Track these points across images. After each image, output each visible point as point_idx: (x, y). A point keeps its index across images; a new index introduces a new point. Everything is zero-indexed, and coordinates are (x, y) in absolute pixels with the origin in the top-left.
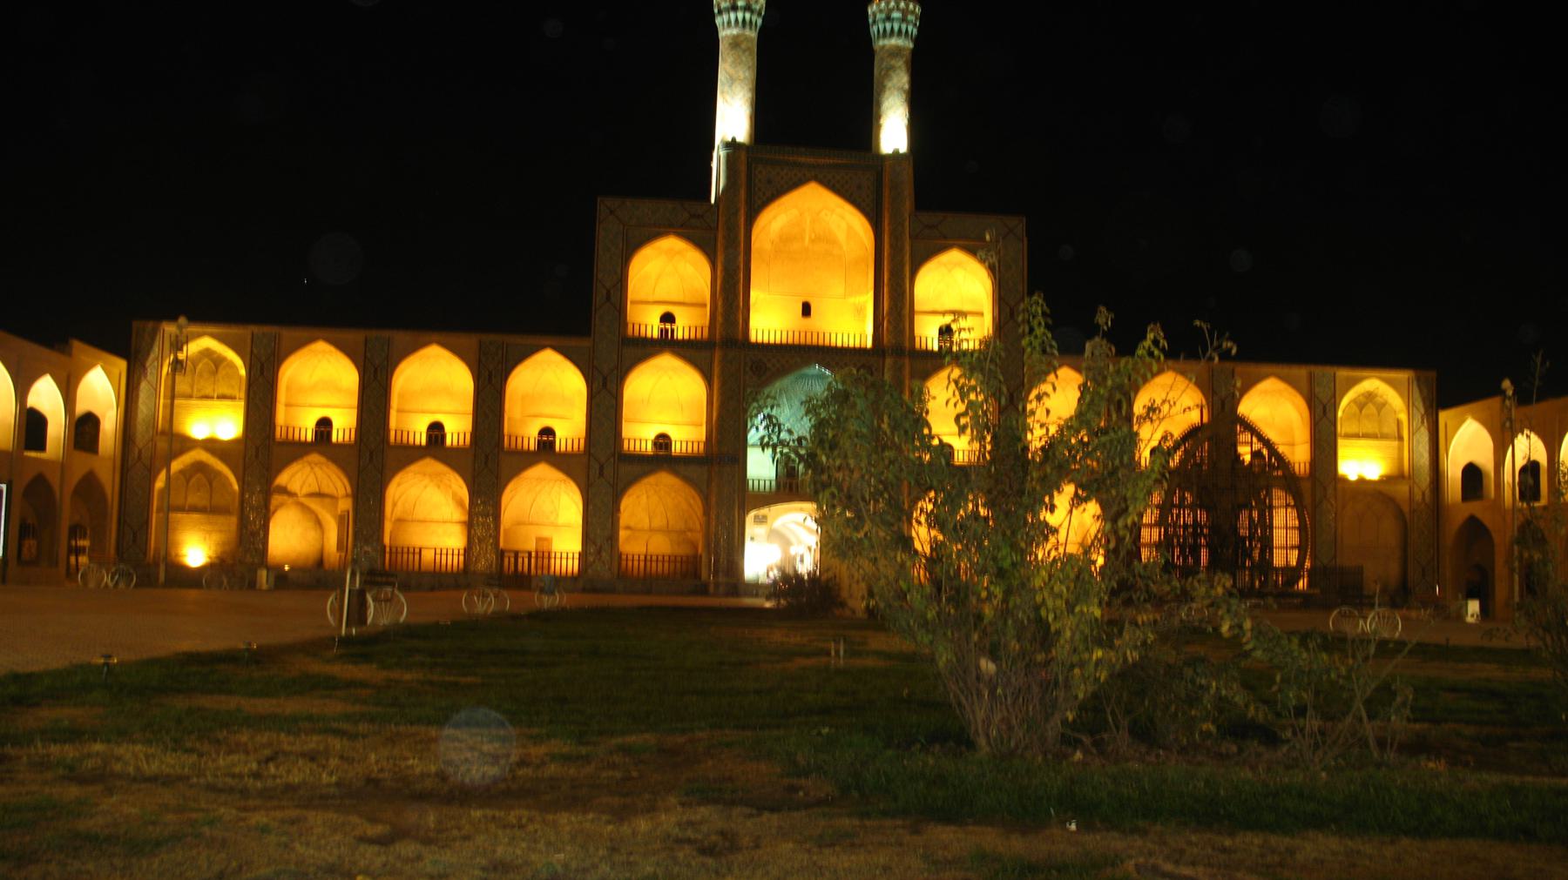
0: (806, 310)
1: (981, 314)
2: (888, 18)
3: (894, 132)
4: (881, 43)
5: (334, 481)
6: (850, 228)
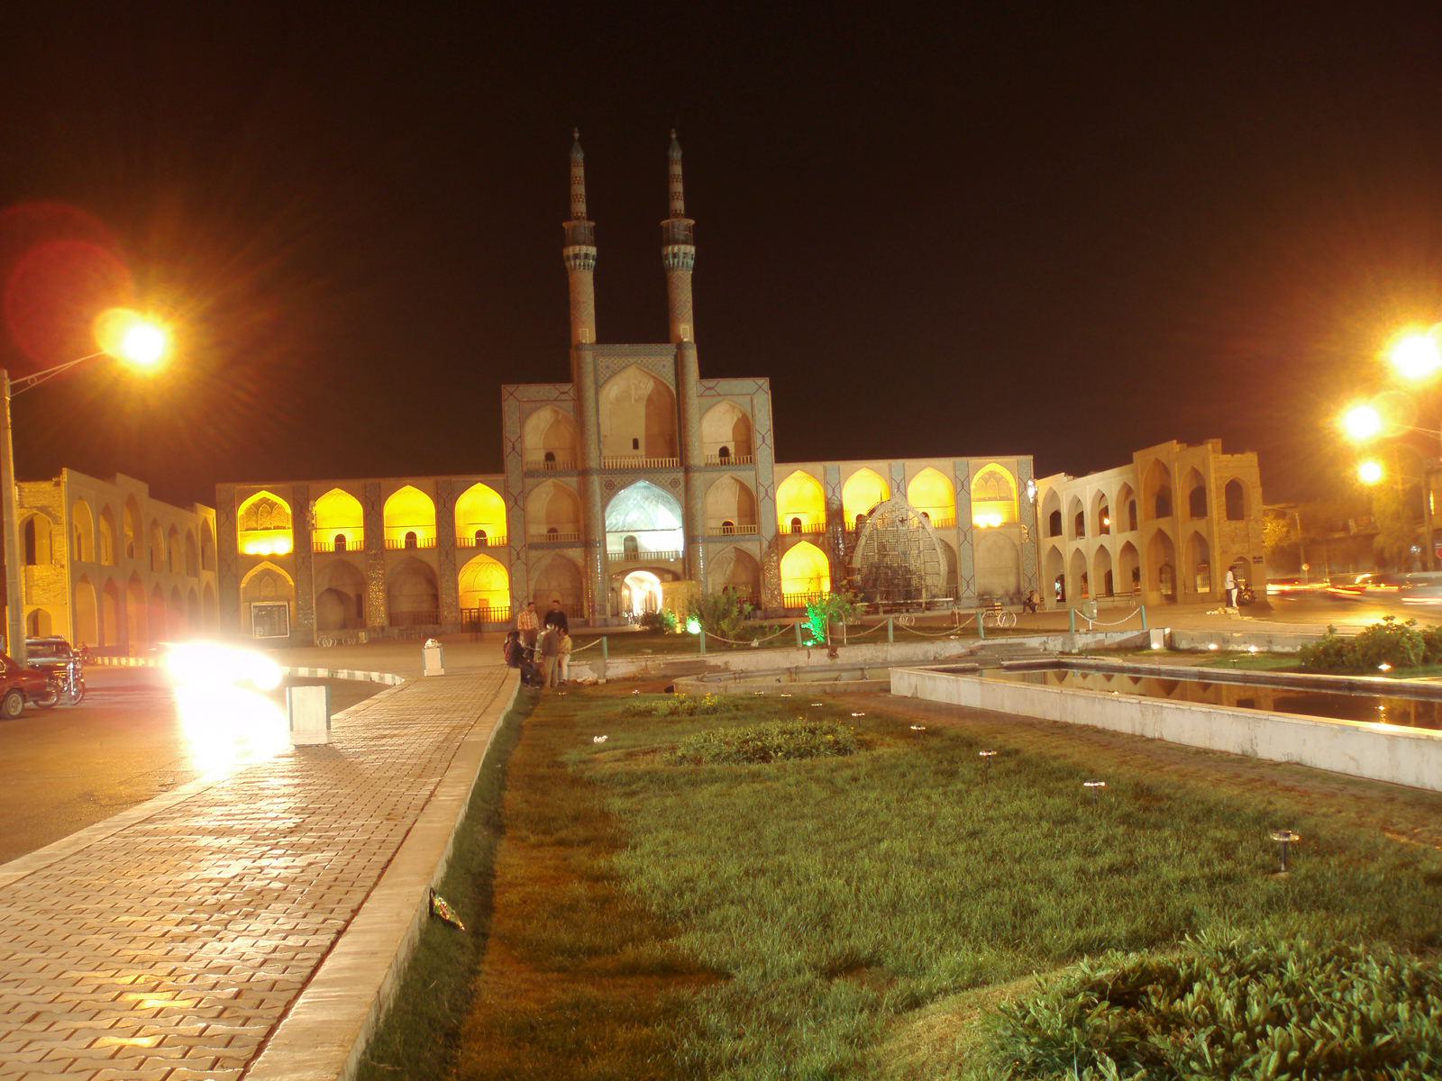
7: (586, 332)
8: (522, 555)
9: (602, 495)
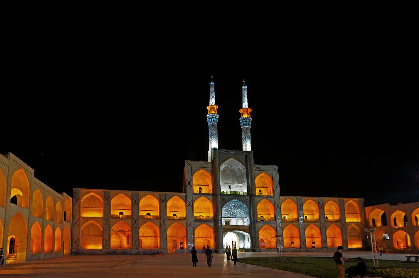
0: (230, 187)
3: (247, 146)
6: (239, 168)
7: (214, 144)
8: (192, 224)
9: (221, 203)
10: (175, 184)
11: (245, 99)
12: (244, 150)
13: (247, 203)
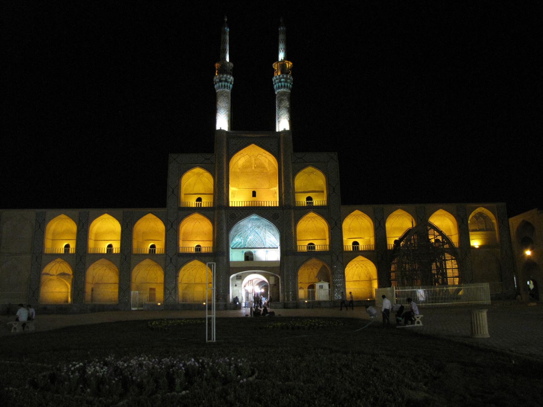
0: (254, 194)
1: (323, 192)
2: (280, 82)
4: (278, 91)
5: (67, 269)
6: (269, 161)
9: (227, 222)
10: (151, 193)
11: (281, 46)
12: (277, 131)
13: (277, 221)
